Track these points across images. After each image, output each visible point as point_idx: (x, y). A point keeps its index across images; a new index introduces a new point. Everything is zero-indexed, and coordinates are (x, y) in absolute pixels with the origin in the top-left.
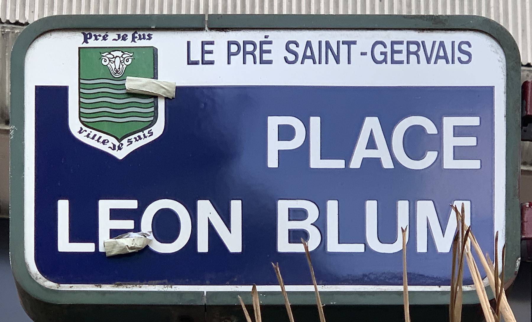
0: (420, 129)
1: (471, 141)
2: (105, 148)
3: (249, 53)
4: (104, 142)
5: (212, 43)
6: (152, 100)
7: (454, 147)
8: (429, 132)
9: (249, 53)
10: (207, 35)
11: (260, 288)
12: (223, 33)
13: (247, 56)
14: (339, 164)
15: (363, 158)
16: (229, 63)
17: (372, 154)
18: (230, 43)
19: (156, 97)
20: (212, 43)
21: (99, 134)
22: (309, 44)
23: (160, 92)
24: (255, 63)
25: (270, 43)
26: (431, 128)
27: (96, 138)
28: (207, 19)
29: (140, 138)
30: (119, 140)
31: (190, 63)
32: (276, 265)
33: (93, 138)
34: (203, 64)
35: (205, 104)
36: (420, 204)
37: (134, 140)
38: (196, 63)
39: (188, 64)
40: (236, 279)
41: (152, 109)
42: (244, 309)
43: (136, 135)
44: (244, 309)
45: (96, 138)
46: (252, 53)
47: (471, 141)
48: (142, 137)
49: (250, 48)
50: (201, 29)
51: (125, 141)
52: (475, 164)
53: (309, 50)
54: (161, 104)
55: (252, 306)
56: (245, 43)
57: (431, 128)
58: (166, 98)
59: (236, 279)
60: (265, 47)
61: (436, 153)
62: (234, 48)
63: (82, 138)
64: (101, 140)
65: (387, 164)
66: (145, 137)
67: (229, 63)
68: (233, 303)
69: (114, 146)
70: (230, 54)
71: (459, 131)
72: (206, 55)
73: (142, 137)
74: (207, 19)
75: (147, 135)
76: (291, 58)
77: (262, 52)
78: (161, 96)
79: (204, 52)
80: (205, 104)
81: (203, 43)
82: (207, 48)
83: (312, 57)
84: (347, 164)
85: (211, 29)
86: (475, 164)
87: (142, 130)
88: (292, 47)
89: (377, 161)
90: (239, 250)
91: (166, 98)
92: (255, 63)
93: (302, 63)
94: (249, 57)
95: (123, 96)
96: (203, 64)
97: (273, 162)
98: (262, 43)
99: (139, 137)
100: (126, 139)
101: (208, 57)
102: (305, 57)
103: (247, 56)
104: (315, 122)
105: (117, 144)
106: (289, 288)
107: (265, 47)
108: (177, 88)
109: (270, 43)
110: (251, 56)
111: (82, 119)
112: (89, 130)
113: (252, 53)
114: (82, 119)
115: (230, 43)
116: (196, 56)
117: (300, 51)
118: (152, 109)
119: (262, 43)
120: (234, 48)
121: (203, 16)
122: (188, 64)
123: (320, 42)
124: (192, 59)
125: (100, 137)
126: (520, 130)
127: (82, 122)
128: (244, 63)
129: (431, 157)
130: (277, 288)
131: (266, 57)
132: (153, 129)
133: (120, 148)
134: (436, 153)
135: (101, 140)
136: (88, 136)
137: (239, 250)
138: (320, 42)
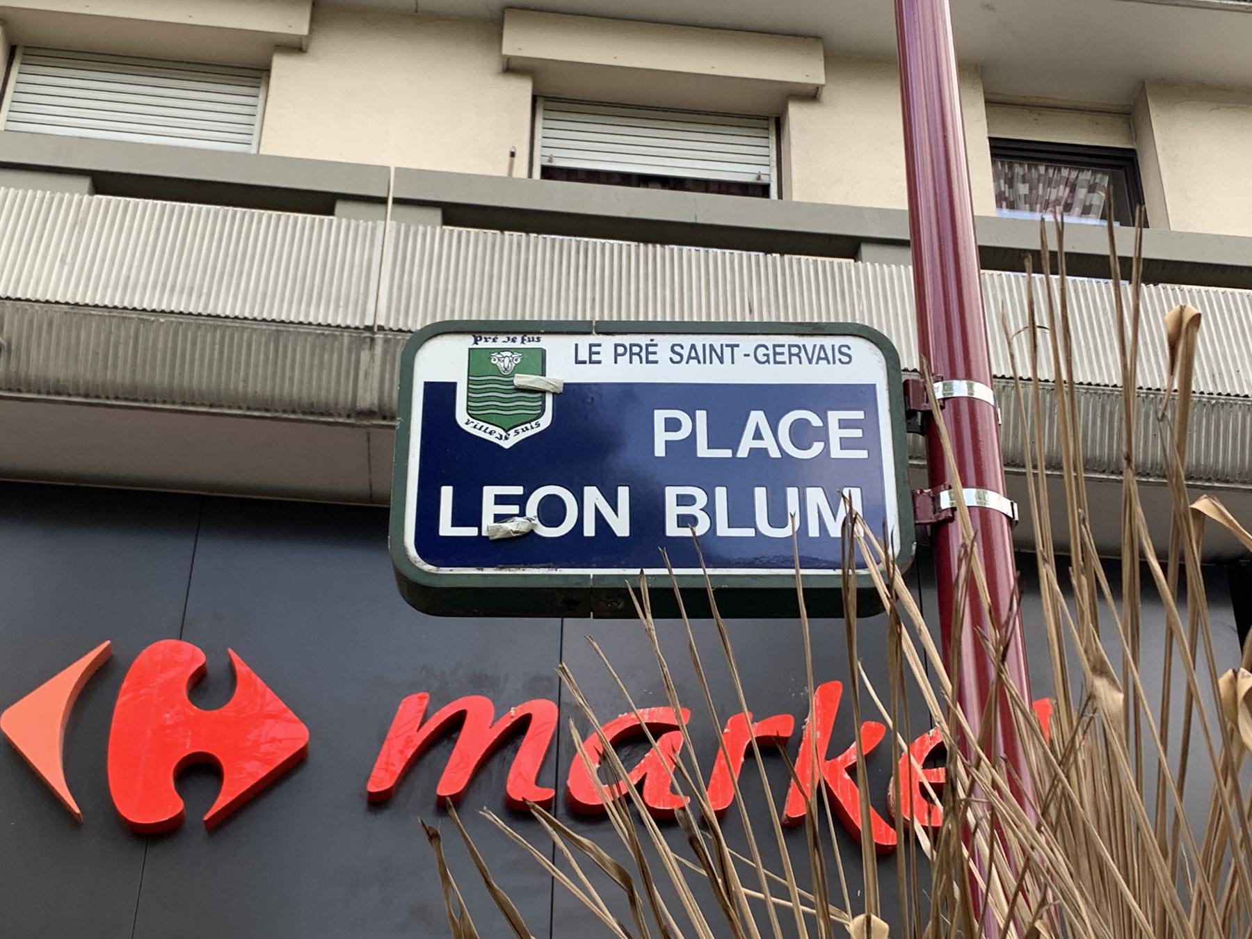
0: (806, 422)
1: (857, 433)
2: (492, 438)
3: (635, 354)
4: (490, 433)
5: (599, 345)
6: (540, 395)
7: (840, 438)
8: (814, 425)
9: (635, 354)
10: (594, 339)
11: (647, 571)
12: (609, 337)
13: (634, 356)
14: (727, 453)
15: (751, 449)
16: (616, 362)
17: (758, 444)
18: (616, 346)
19: (544, 392)
20: (599, 345)
21: (486, 425)
22: (693, 347)
23: (548, 388)
24: (641, 362)
25: (656, 345)
26: (816, 421)
27: (483, 429)
28: (594, 324)
29: (527, 429)
30: (506, 431)
31: (577, 362)
32: (662, 548)
33: (480, 429)
34: (590, 363)
35: (593, 399)
36: (810, 492)
37: (521, 431)
38: (584, 362)
39: (576, 363)
40: (623, 563)
41: (540, 403)
42: (632, 593)
43: (523, 427)
44: (632, 593)
45: (483, 429)
46: (638, 354)
47: (857, 433)
48: (529, 427)
49: (636, 350)
50: (589, 333)
51: (512, 432)
52: (863, 454)
53: (693, 351)
54: (549, 399)
55: (639, 589)
56: (631, 345)
57: (816, 421)
58: (554, 394)
59: (623, 563)
60: (651, 349)
61: (822, 444)
62: (620, 350)
63: (469, 429)
64: (488, 431)
65: (774, 453)
66: (532, 428)
67: (616, 362)
68: (620, 586)
69: (501, 436)
70: (616, 355)
71: (844, 424)
72: (593, 356)
73: (529, 427)
74: (594, 324)
75: (534, 426)
76: (677, 358)
77: (648, 353)
78: (549, 392)
79: (591, 353)
80: (593, 399)
81: (591, 346)
82: (594, 349)
83: (697, 358)
84: (734, 453)
85: (598, 333)
86: (863, 454)
87: (529, 422)
88: (677, 349)
89: (764, 451)
90: (627, 534)
91: (554, 394)
92: (641, 362)
93: (687, 363)
94: (636, 358)
95: (510, 392)
96: (590, 363)
97: (660, 451)
98: (647, 346)
99: (526, 428)
100: (513, 431)
101: (595, 357)
102: (690, 358)
103: (634, 356)
104: (701, 415)
105: (504, 434)
106: (676, 571)
107: (651, 349)
108: (565, 384)
109: (656, 345)
110: (637, 357)
111: (470, 412)
112: (476, 422)
113: (638, 354)
114: (470, 412)
115: (616, 346)
116: (584, 355)
117: (685, 353)
118: (540, 403)
119: (647, 346)
120: (620, 350)
121: (592, 322)
122: (576, 363)
123: (704, 345)
124: (580, 359)
125: (487, 428)
126: (904, 424)
127: (469, 414)
128: (631, 362)
129: (818, 447)
130: (664, 571)
131: (651, 357)
132: (540, 421)
133: (506, 438)
134: (822, 444)
135: (488, 431)
136: (475, 427)
137: (627, 534)
138: (704, 345)
